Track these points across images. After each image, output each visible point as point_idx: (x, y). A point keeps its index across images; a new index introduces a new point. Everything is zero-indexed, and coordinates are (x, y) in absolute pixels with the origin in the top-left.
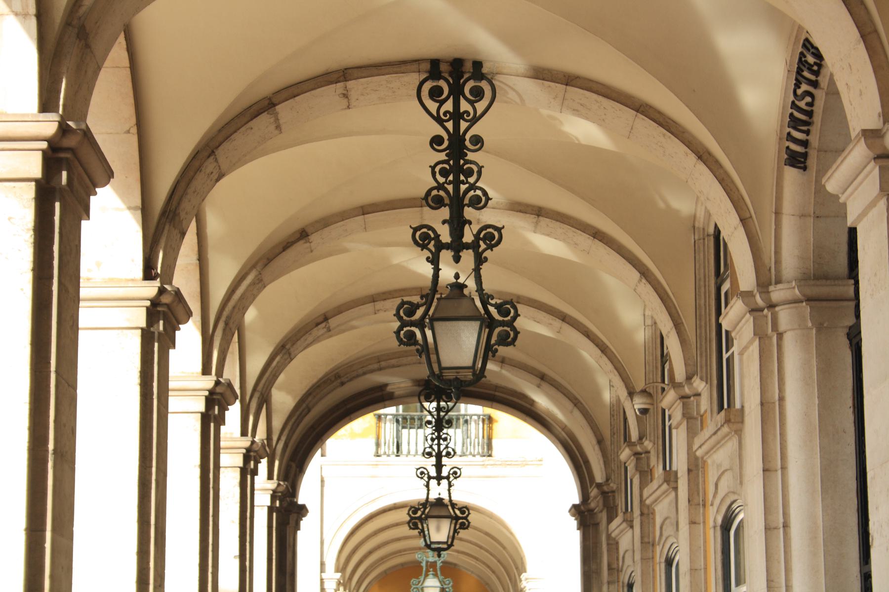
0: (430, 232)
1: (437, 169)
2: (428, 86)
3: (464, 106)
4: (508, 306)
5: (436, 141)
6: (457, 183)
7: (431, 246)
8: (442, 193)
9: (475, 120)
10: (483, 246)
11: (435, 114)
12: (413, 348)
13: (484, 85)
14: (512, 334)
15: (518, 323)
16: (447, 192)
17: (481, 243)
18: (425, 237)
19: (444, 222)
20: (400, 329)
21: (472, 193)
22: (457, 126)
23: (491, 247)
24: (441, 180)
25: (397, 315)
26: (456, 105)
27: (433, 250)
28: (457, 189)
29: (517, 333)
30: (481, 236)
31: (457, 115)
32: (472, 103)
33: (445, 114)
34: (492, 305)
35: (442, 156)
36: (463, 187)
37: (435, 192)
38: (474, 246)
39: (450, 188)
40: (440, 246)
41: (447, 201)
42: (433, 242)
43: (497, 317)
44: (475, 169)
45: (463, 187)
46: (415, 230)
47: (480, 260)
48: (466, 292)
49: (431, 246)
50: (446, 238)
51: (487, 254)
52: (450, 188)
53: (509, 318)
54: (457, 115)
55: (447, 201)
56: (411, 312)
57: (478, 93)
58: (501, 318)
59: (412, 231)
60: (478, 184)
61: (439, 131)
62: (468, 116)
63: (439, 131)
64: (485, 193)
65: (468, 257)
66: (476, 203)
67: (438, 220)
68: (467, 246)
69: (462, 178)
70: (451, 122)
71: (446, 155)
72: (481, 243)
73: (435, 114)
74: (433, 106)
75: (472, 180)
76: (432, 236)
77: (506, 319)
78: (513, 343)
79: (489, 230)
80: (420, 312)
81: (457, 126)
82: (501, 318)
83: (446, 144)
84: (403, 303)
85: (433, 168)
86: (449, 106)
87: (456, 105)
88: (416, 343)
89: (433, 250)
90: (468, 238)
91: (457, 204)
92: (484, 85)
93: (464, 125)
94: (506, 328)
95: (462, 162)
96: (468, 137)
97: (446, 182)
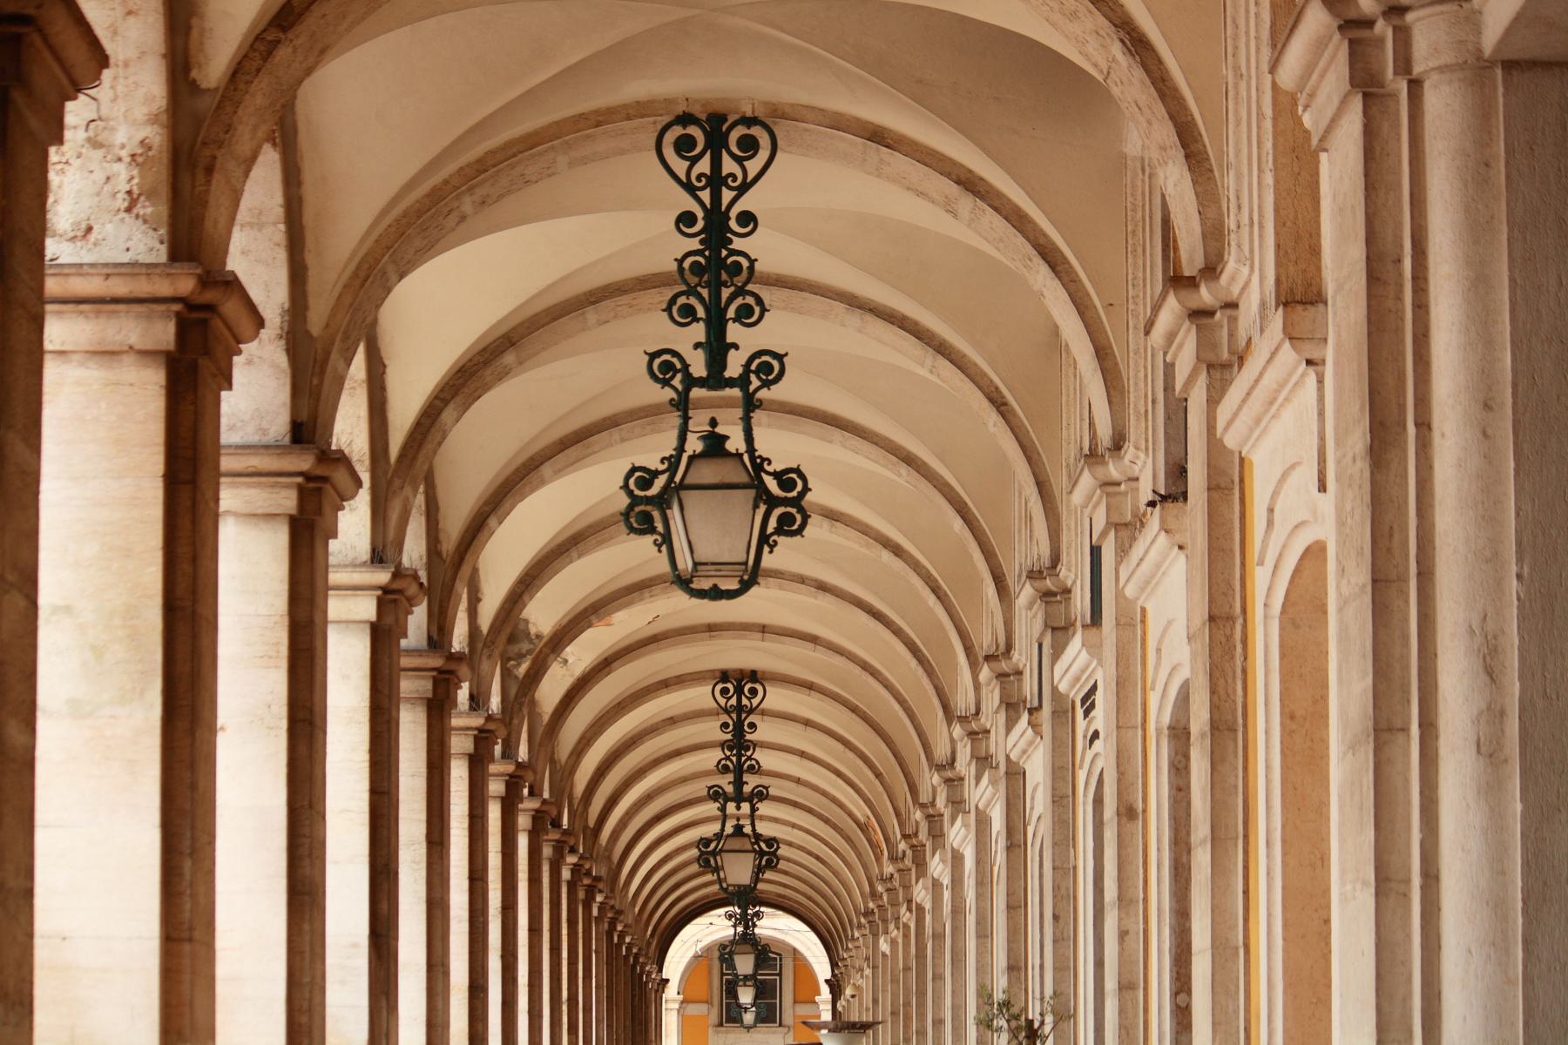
0: (675, 360)
2: (677, 131)
3: (729, 166)
4: (794, 476)
5: (686, 219)
7: (677, 382)
8: (693, 301)
9: (744, 188)
10: (755, 383)
11: (684, 178)
17: (753, 377)
19: (697, 346)
20: (631, 507)
21: (739, 301)
22: (716, 197)
23: (767, 384)
24: (693, 280)
26: (716, 164)
27: (680, 387)
30: (753, 367)
31: (716, 181)
32: (739, 161)
34: (768, 473)
36: (726, 293)
37: (682, 300)
38: (742, 381)
39: (705, 293)
41: (701, 313)
42: (679, 376)
44: (745, 263)
45: (726, 293)
50: (699, 369)
51: (763, 394)
52: (705, 293)
53: (794, 494)
54: (716, 181)
55: (701, 313)
56: (646, 484)
58: (782, 494)
60: (750, 287)
62: (735, 179)
64: (759, 301)
66: (744, 314)
67: (688, 340)
68: (731, 383)
69: (724, 276)
70: (708, 191)
71: (701, 242)
72: (753, 377)
73: (684, 178)
74: (680, 166)
75: (739, 280)
76: (679, 366)
79: (765, 358)
80: (660, 482)
81: (716, 197)
83: (700, 225)
84: (634, 469)
86: (704, 166)
87: (716, 164)
89: (680, 387)
90: (734, 369)
92: (756, 131)
93: (727, 195)
94: (789, 509)
95: (724, 253)
97: (699, 284)
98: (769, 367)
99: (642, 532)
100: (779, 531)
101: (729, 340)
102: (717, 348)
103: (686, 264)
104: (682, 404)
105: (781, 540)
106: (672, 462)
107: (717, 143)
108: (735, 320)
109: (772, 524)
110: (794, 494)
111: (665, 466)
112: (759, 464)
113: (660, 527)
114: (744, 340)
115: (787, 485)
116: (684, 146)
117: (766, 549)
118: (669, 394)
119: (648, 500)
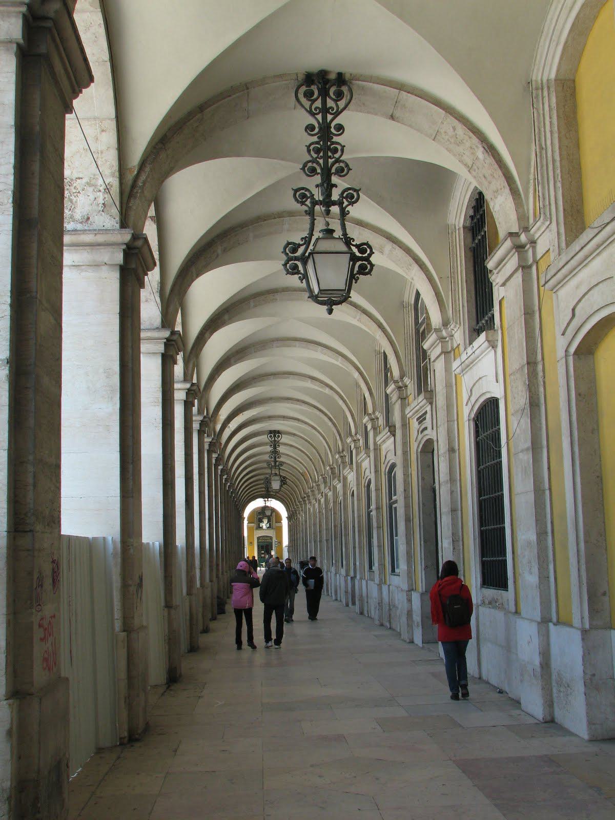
1: (311, 148)
2: (304, 89)
4: (366, 246)
5: (310, 128)
6: (326, 158)
7: (308, 202)
8: (315, 165)
10: (346, 203)
12: (296, 276)
13: (345, 89)
14: (369, 266)
15: (372, 259)
16: (318, 163)
17: (344, 200)
18: (304, 196)
19: (317, 186)
21: (337, 165)
22: (325, 118)
23: (352, 204)
25: (284, 252)
26: (324, 103)
28: (326, 162)
29: (372, 266)
30: (344, 195)
32: (336, 101)
33: (316, 109)
34: (353, 245)
35: (315, 139)
36: (330, 161)
39: (321, 161)
40: (314, 203)
42: (309, 200)
43: (358, 254)
44: (339, 147)
46: (296, 191)
47: (344, 214)
48: (335, 235)
49: (308, 202)
51: (349, 208)
52: (321, 161)
53: (366, 255)
54: (325, 110)
56: (294, 250)
57: (339, 95)
58: (360, 255)
59: (293, 192)
60: (341, 159)
61: (311, 120)
62: (333, 110)
63: (311, 120)
64: (347, 165)
65: (335, 209)
67: (313, 183)
68: (334, 203)
71: (319, 138)
72: (344, 200)
74: (307, 104)
75: (337, 156)
76: (309, 195)
77: (364, 256)
78: (369, 273)
80: (301, 250)
81: (325, 118)
82: (360, 255)
83: (317, 130)
84: (289, 243)
85: (308, 147)
87: (324, 103)
88: (298, 273)
90: (335, 196)
91: (327, 175)
93: (329, 117)
94: (364, 262)
95: (329, 143)
96: (333, 125)
98: (351, 196)
99: (293, 274)
100: (360, 273)
101: (333, 182)
102: (328, 186)
103: (311, 148)
104: (311, 213)
105: (361, 277)
106: (307, 241)
107: (324, 94)
108: (335, 174)
109: (356, 269)
110: (366, 255)
111: (303, 242)
112: (348, 241)
113: (302, 271)
114: (340, 183)
115: (362, 251)
116: (309, 95)
117: (354, 281)
118: (306, 208)
119: (296, 259)
